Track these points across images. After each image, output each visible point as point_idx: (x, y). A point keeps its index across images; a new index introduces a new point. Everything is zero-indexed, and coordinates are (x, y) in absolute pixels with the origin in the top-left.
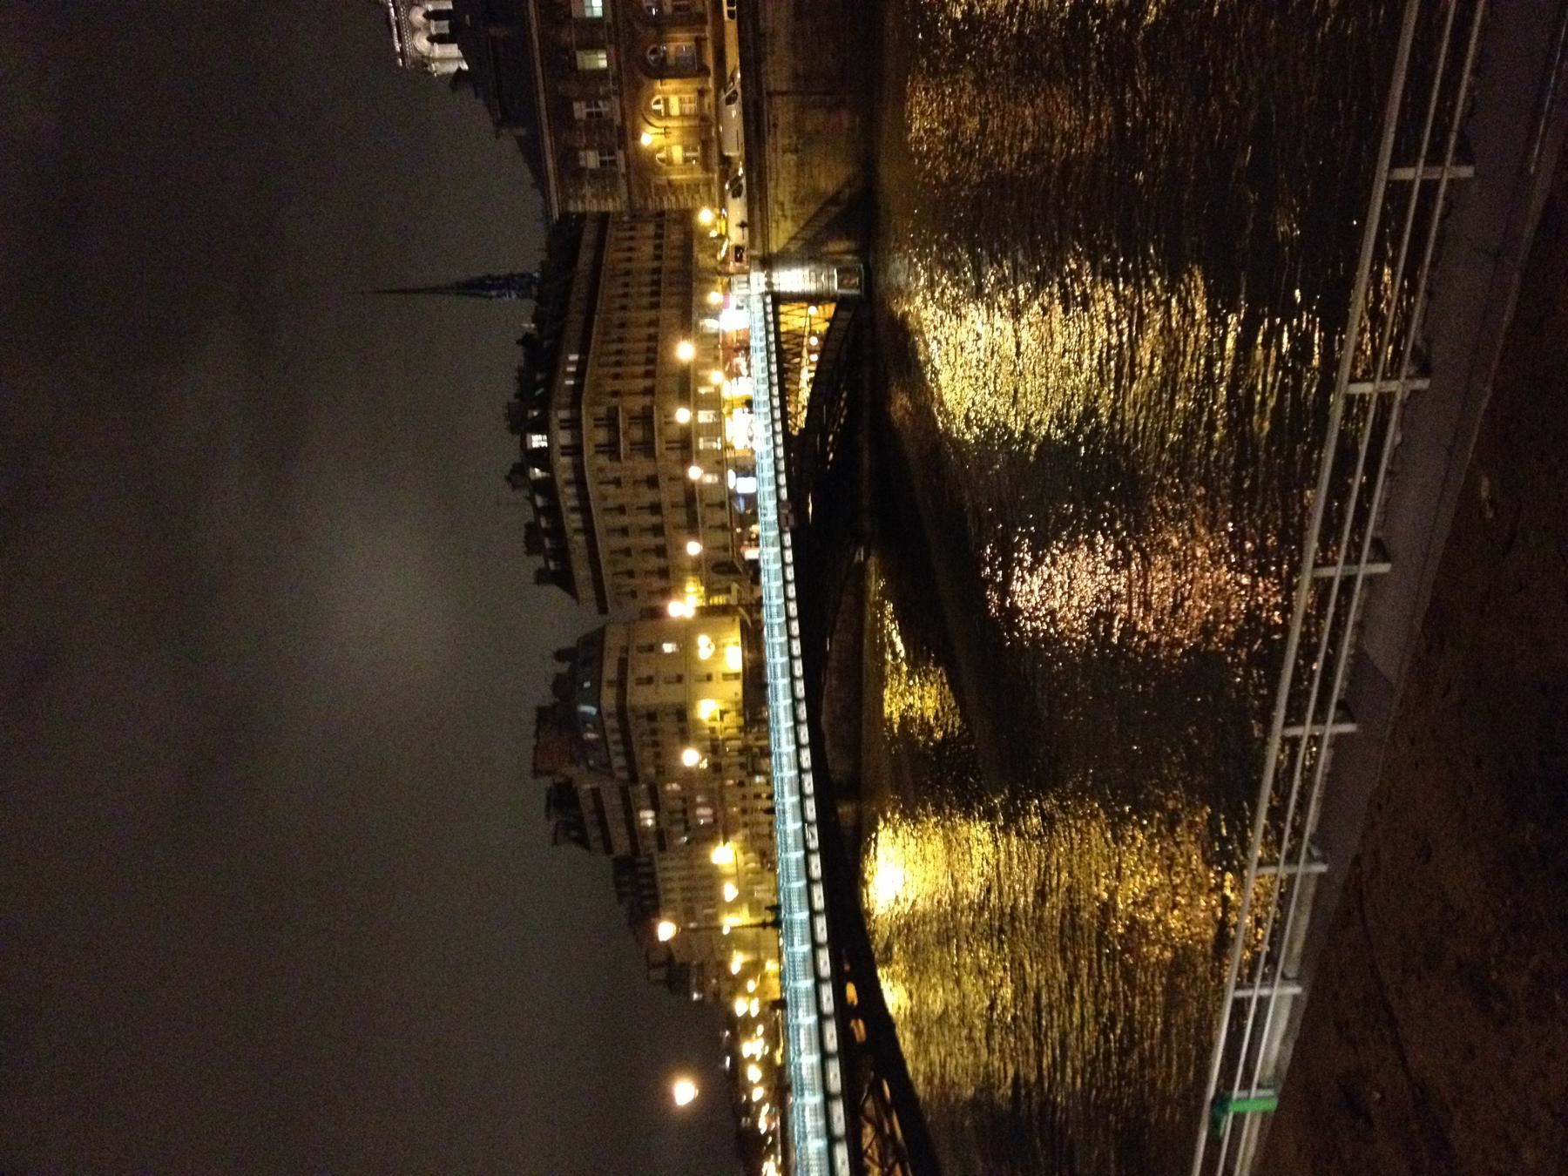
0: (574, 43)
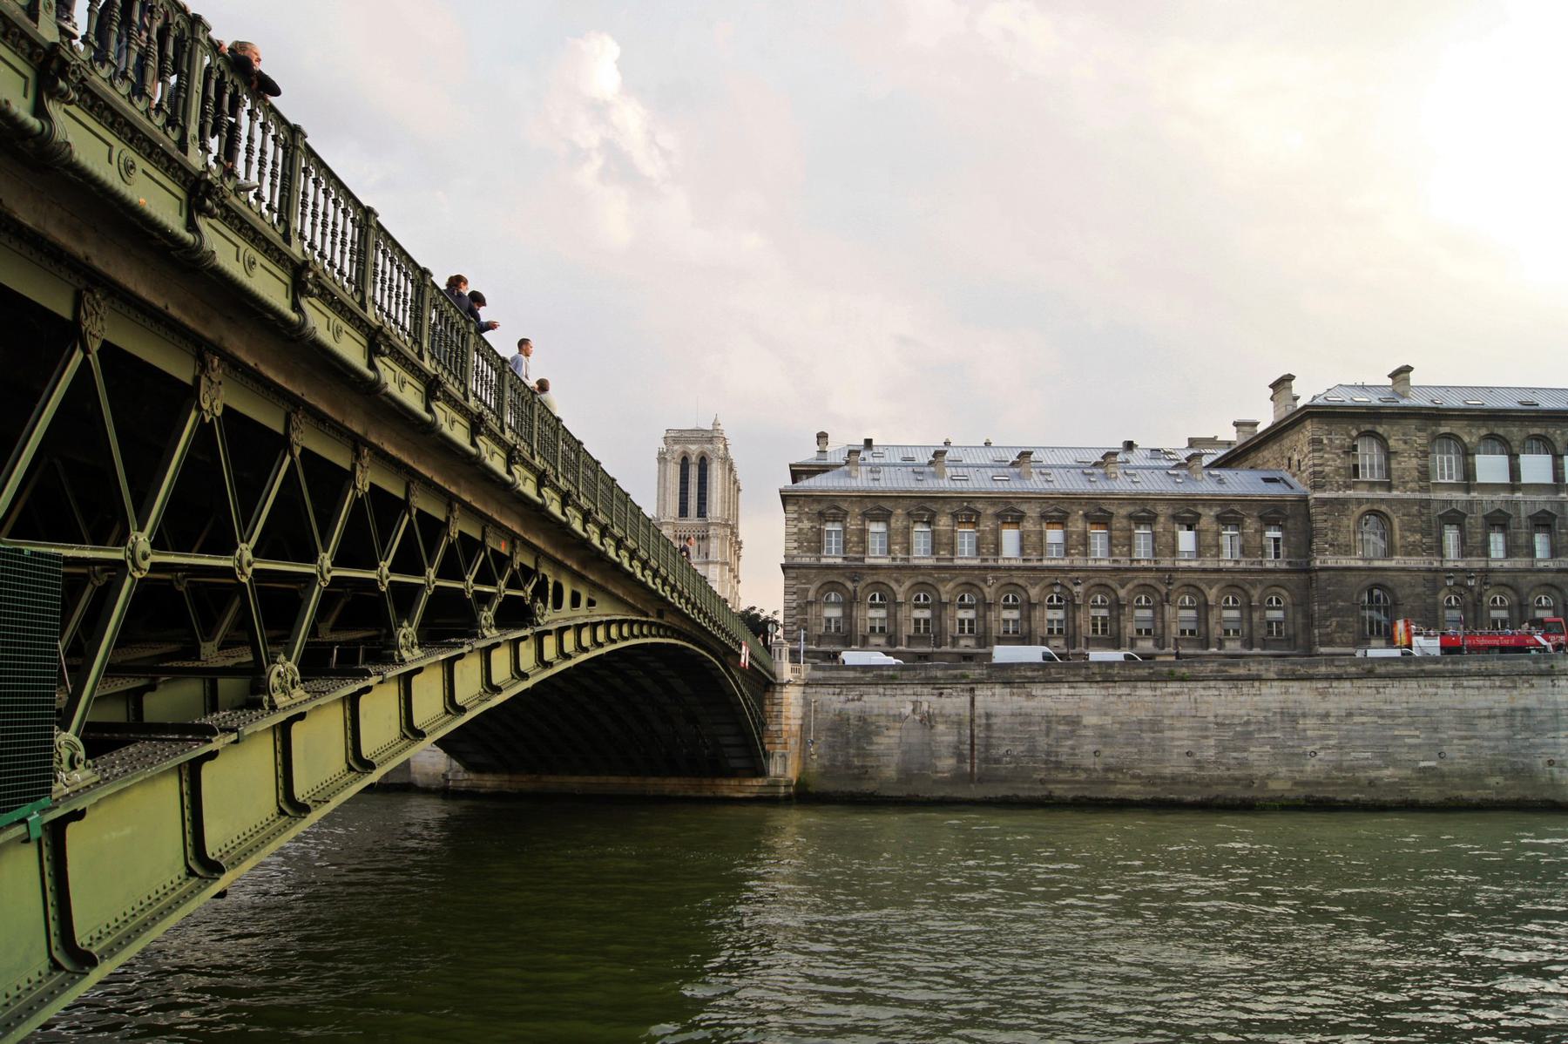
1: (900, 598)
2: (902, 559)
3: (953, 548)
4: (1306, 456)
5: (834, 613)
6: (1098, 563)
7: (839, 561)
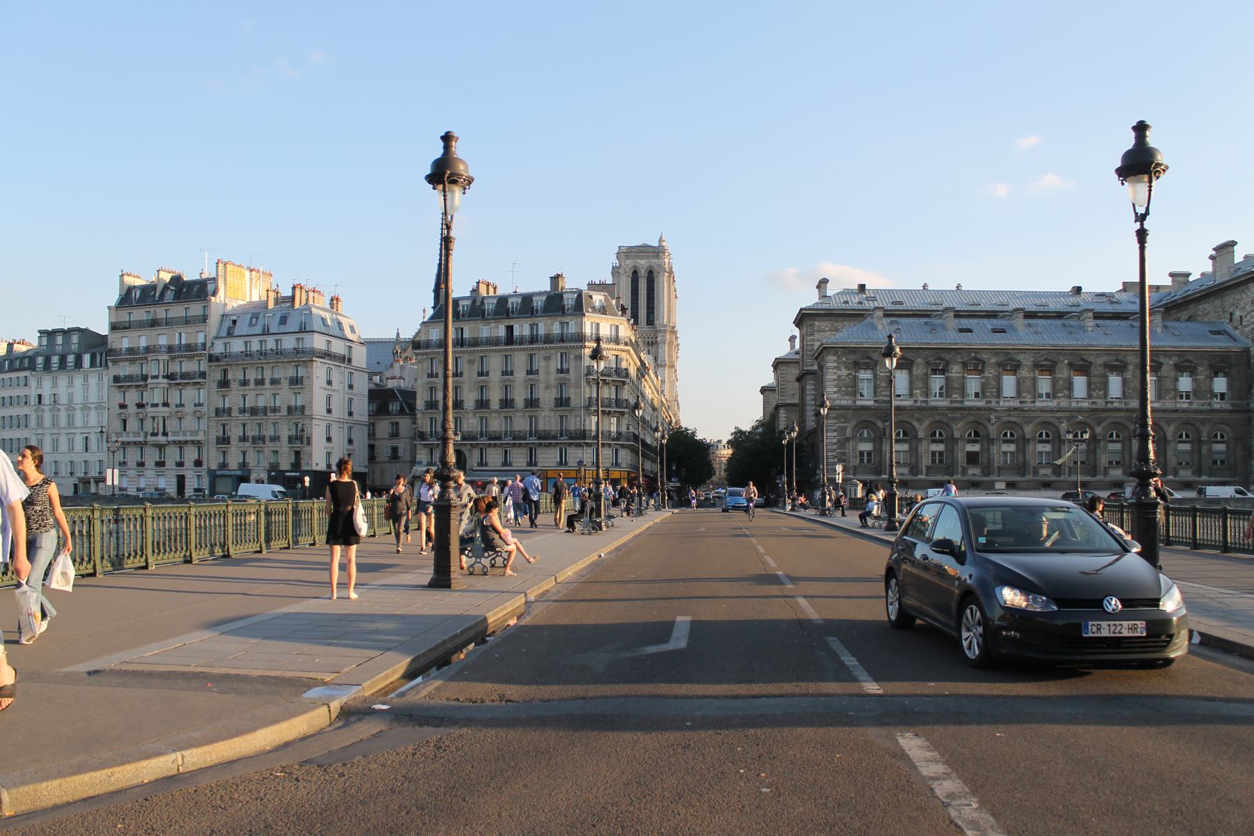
0: (950, 375)
1: (921, 435)
2: (922, 402)
3: (963, 392)
4: (1248, 314)
5: (867, 447)
6: (1080, 405)
7: (871, 403)
